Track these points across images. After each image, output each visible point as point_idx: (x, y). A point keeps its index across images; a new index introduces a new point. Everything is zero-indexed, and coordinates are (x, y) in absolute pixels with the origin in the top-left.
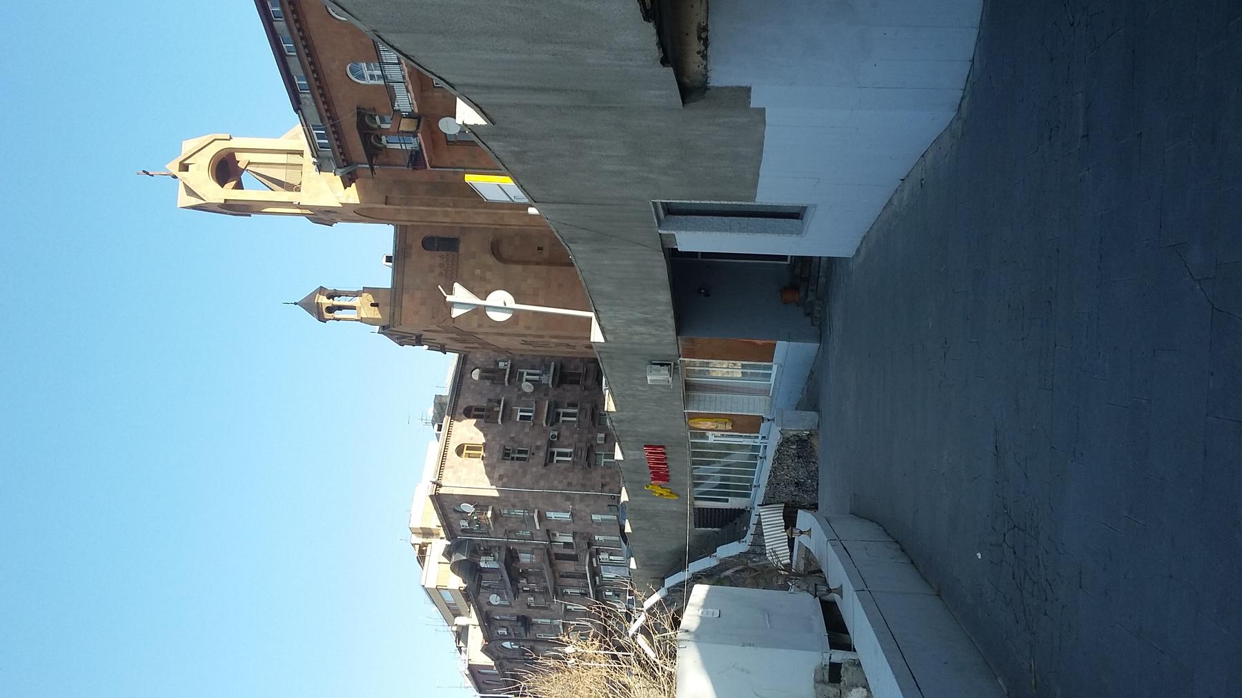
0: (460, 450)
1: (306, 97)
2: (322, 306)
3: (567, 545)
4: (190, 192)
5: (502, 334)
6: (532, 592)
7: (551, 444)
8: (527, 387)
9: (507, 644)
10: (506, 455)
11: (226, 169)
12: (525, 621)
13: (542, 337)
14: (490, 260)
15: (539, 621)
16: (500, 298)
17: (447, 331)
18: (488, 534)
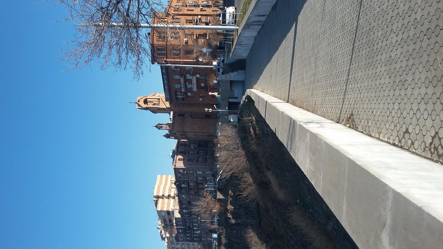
0: (179, 160)
1: (167, 90)
2: (159, 127)
3: (201, 180)
4: (139, 105)
5: (191, 132)
6: (192, 194)
7: (198, 158)
8: (192, 147)
9: (184, 211)
10: (189, 160)
11: (146, 102)
12: (189, 203)
13: (198, 132)
14: (190, 118)
15: (193, 203)
16: (210, 109)
17: (182, 132)
18: (184, 178)
